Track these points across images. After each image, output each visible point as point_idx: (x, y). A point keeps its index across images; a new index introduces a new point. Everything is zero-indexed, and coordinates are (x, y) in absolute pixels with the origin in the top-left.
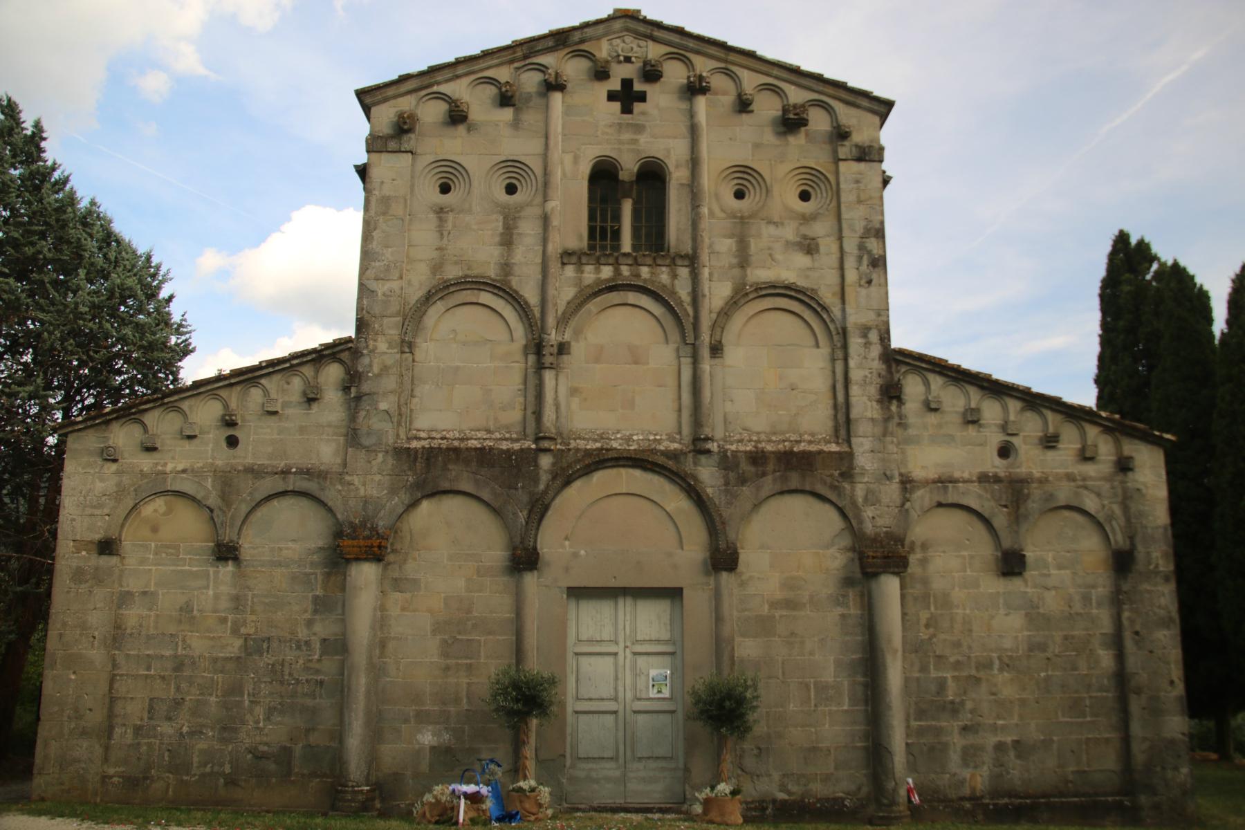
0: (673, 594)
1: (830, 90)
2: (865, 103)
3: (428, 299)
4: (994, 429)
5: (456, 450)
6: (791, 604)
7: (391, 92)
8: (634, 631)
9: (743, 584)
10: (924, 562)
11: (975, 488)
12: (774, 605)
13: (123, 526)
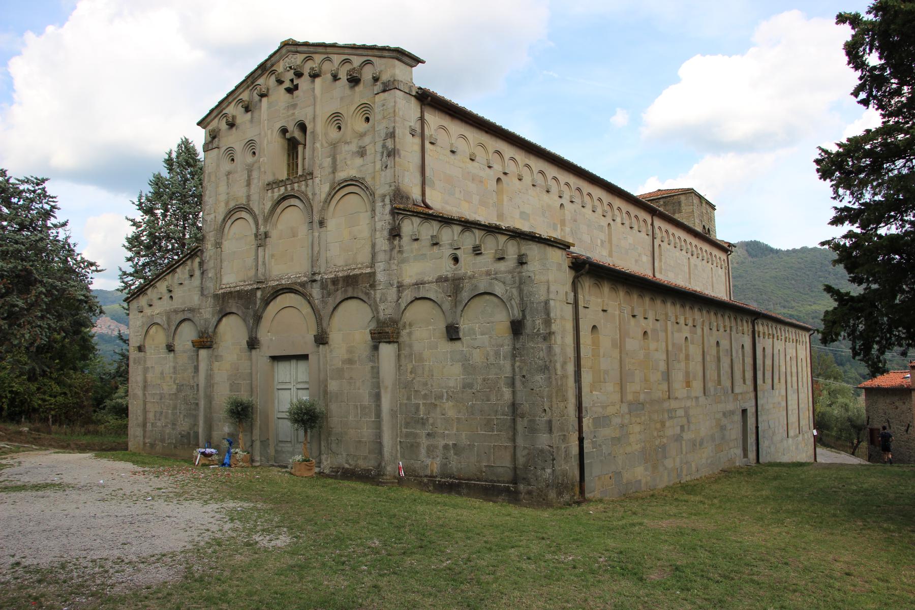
0: (305, 357)
1: (370, 52)
2: (386, 54)
3: (224, 221)
4: (448, 247)
5: (231, 293)
6: (350, 361)
7: (209, 119)
8: (297, 377)
9: (331, 351)
10: (410, 334)
12: (344, 362)
13: (145, 339)
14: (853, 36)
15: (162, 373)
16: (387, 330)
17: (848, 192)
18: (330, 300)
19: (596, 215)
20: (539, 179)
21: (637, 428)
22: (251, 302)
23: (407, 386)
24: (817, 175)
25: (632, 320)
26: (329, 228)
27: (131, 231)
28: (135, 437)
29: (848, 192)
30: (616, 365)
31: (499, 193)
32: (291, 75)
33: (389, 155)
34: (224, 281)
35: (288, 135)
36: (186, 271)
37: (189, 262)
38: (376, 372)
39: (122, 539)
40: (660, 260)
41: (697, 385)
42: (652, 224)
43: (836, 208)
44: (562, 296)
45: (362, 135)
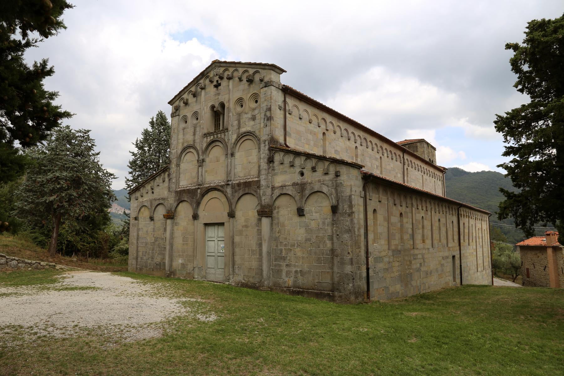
0: (222, 224)
1: (258, 67)
2: (267, 67)
3: (182, 153)
5: (184, 190)
6: (246, 226)
7: (174, 101)
10: (278, 212)
11: (291, 188)
12: (243, 227)
14: (515, 55)
15: (147, 232)
16: (266, 210)
17: (512, 138)
18: (236, 194)
19: (374, 152)
20: (345, 133)
21: (397, 264)
22: (195, 195)
23: (276, 239)
24: (495, 130)
25: (394, 207)
26: (236, 157)
27: (132, 158)
28: (132, 265)
29: (512, 138)
30: (386, 230)
31: (324, 140)
32: (217, 78)
33: (268, 120)
34: (181, 184)
35: (215, 109)
36: (161, 179)
37: (163, 174)
38: (259, 232)
39: (129, 315)
40: (407, 176)
41: (428, 242)
42: (403, 157)
43: (506, 147)
44: (358, 193)
45: (254, 109)
